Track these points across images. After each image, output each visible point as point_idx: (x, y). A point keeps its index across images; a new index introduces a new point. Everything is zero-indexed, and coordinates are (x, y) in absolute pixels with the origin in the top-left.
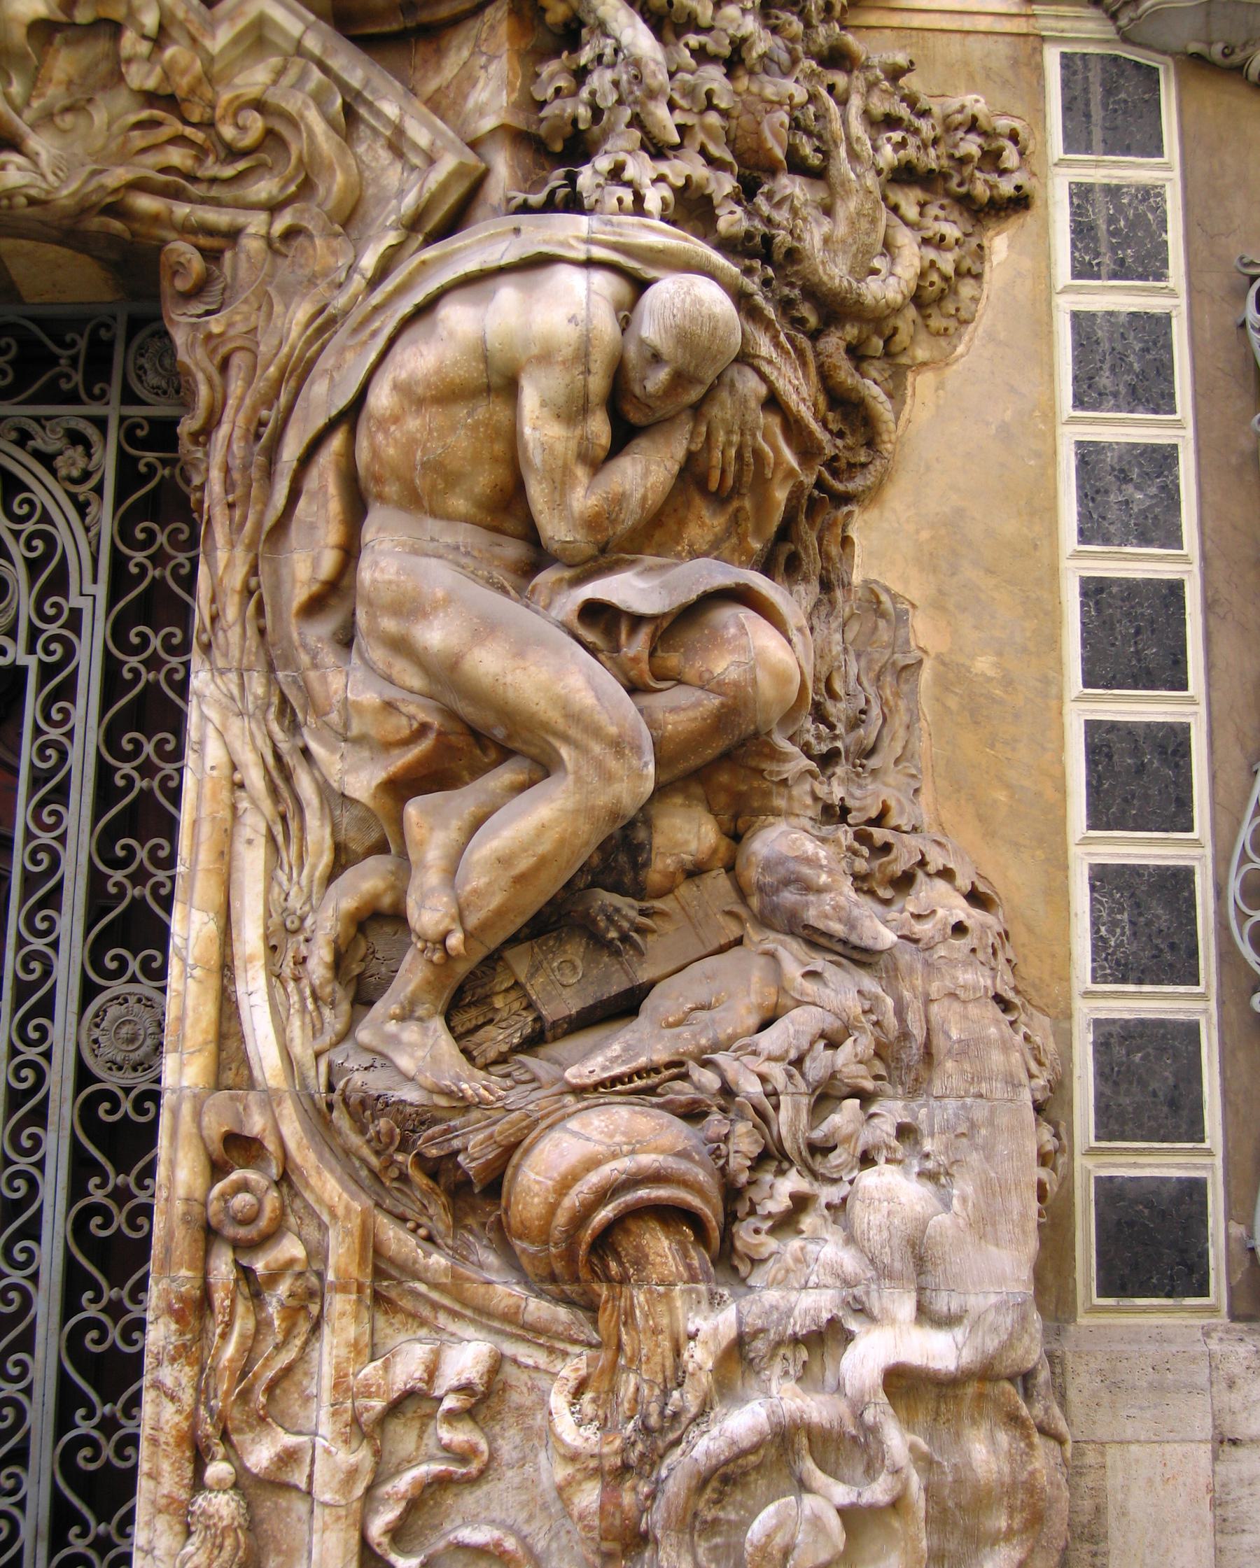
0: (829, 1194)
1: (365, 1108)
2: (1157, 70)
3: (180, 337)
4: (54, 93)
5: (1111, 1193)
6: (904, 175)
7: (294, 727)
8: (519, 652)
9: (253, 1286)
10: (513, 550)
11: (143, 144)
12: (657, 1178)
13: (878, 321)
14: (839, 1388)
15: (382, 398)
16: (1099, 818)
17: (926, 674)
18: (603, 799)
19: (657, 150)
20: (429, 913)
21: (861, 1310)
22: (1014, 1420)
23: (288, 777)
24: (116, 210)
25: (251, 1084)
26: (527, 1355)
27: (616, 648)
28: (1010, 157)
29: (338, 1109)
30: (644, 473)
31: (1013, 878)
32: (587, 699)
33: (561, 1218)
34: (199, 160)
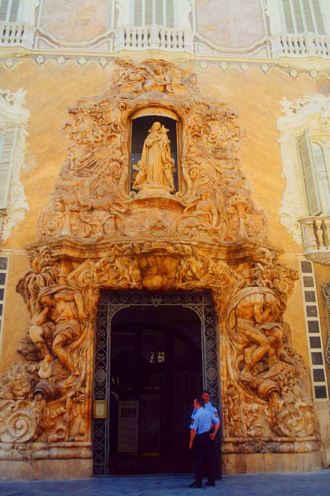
0: (290, 389)
1: (243, 381)
2: (310, 263)
3: (215, 299)
5: (316, 387)
6: (287, 277)
7: (232, 341)
8: (257, 334)
9: (233, 400)
10: (253, 322)
12: (274, 388)
13: (285, 294)
14: (294, 408)
15: (239, 307)
16: (312, 347)
17: (292, 332)
18: (266, 349)
19: (264, 279)
20: (248, 361)
21: (295, 400)
22: (311, 411)
23: (231, 347)
25: (230, 379)
26: (261, 406)
27: (265, 333)
28: (297, 274)
29: (241, 381)
30: (266, 314)
31: (303, 354)
32: (264, 339)
33: (265, 392)
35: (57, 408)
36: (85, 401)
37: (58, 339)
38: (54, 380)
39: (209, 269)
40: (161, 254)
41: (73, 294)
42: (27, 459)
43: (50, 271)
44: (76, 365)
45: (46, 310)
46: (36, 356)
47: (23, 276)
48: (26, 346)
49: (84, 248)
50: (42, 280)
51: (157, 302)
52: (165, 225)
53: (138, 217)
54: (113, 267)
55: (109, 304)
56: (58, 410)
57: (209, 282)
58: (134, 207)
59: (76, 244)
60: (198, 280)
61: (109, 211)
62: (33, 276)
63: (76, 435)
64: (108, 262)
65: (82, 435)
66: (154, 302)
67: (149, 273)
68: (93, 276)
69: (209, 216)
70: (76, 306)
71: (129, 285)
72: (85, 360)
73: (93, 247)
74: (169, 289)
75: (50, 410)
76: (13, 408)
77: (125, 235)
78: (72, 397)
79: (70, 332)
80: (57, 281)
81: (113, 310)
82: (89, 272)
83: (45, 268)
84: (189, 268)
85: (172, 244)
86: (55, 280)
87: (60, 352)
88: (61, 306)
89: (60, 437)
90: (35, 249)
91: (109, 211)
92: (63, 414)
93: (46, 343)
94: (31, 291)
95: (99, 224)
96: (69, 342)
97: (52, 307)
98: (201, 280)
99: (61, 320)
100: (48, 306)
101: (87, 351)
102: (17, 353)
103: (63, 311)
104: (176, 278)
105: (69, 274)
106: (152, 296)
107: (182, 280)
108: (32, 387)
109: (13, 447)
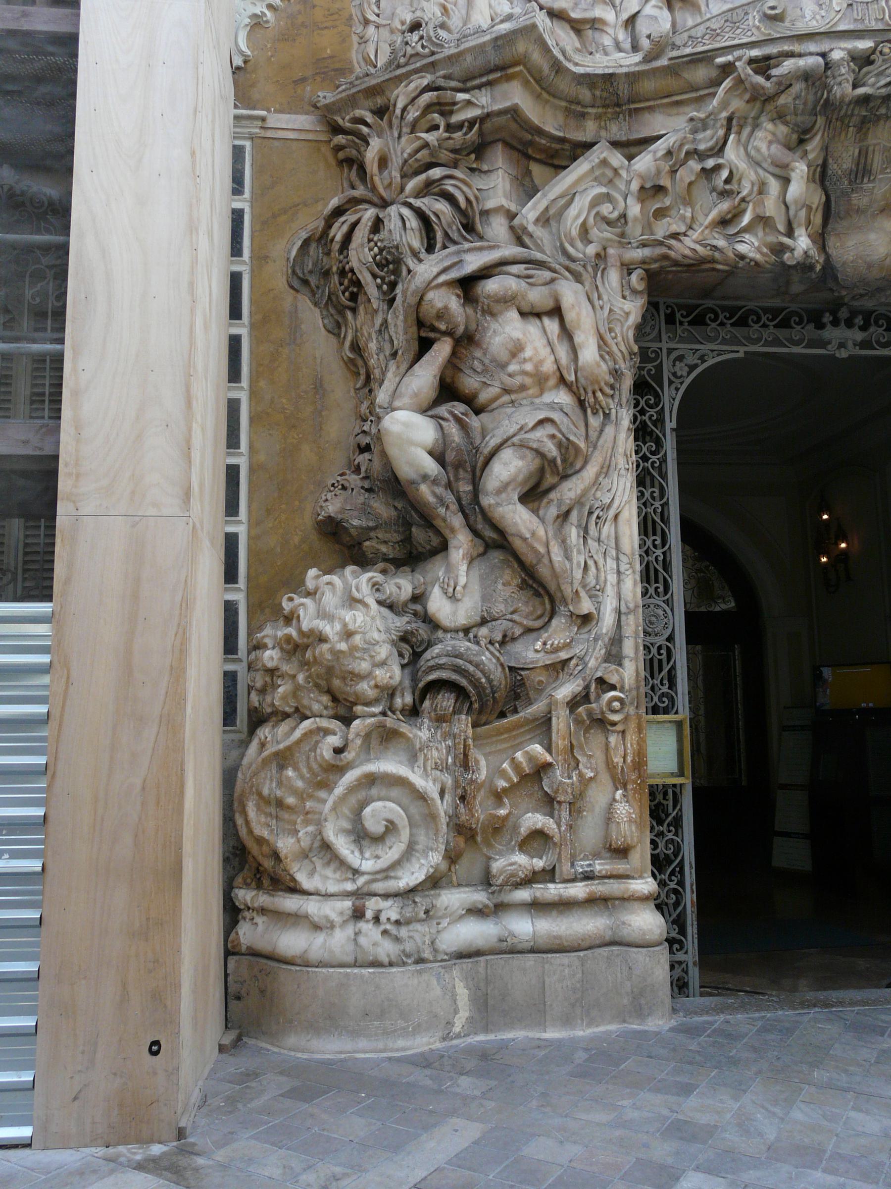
35: (517, 748)
36: (626, 719)
37: (508, 468)
38: (499, 638)
41: (553, 280)
42: (420, 961)
43: (449, 186)
44: (578, 574)
45: (442, 350)
46: (408, 539)
47: (322, 224)
48: (361, 499)
49: (585, 94)
50: (413, 222)
51: (843, 342)
54: (709, 174)
55: (664, 346)
56: (519, 755)
59: (558, 68)
62: (369, 214)
63: (596, 855)
65: (622, 852)
66: (835, 343)
68: (624, 216)
70: (567, 333)
71: (779, 249)
72: (614, 553)
73: (624, 90)
75: (486, 756)
76: (338, 751)
78: (573, 704)
79: (553, 437)
80: (479, 227)
81: (681, 369)
82: (608, 198)
83: (423, 177)
86: (469, 227)
87: (519, 518)
88: (509, 328)
89: (539, 864)
90: (369, 103)
92: (541, 770)
93: (449, 486)
94: (366, 278)
95: (609, 15)
96: (550, 479)
97: (466, 341)
99: (506, 391)
100: (449, 333)
101: (616, 517)
102: (314, 537)
103: (516, 350)
105: (524, 206)
106: (827, 318)
108: (403, 666)
109: (358, 914)
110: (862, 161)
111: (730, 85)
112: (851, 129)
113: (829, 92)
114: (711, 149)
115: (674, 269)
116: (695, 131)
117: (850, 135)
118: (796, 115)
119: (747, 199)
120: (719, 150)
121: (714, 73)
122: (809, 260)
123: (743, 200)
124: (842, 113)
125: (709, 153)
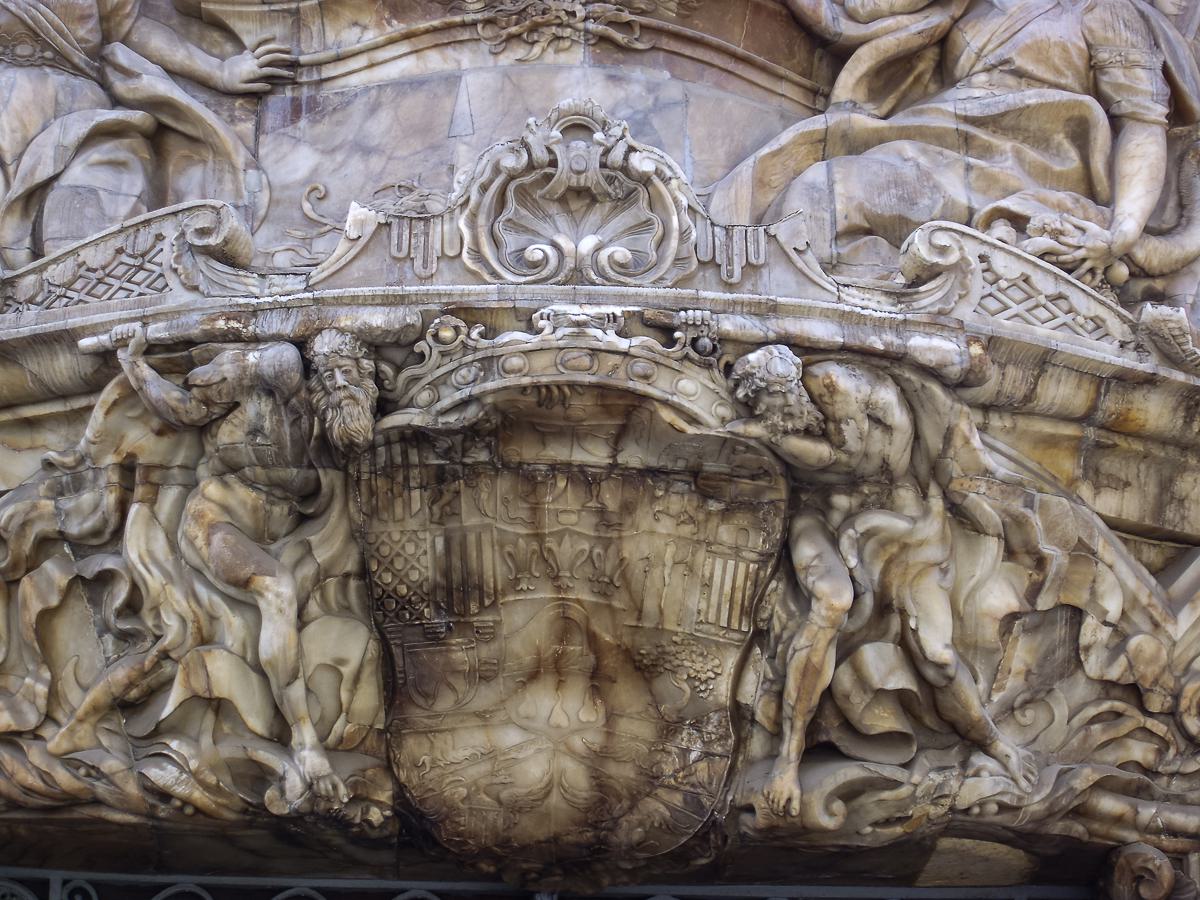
4: (1013, 683)
11: (1104, 738)
24: (1080, 812)
34: (1161, 753)
39: (1093, 632)
40: (595, 455)
52: (642, 163)
53: (379, 128)
57: (1085, 777)
58: (351, 38)
60: (971, 740)
61: (98, 68)
64: (46, 544)
67: (461, 654)
69: (1080, 134)
71: (261, 777)
74: (669, 828)
77: (226, 256)
84: (885, 606)
85: (718, 354)
91: (98, 68)
98: (1007, 742)
104: (739, 715)
107: (812, 729)
110: (456, 562)
111: (115, 396)
112: (416, 494)
113: (323, 421)
114: (96, 533)
115: (18, 815)
116: (58, 492)
117: (416, 506)
118: (264, 466)
119: (173, 655)
120: (112, 536)
121: (87, 367)
122: (322, 805)
123: (165, 655)
124: (382, 460)
125: (95, 542)
